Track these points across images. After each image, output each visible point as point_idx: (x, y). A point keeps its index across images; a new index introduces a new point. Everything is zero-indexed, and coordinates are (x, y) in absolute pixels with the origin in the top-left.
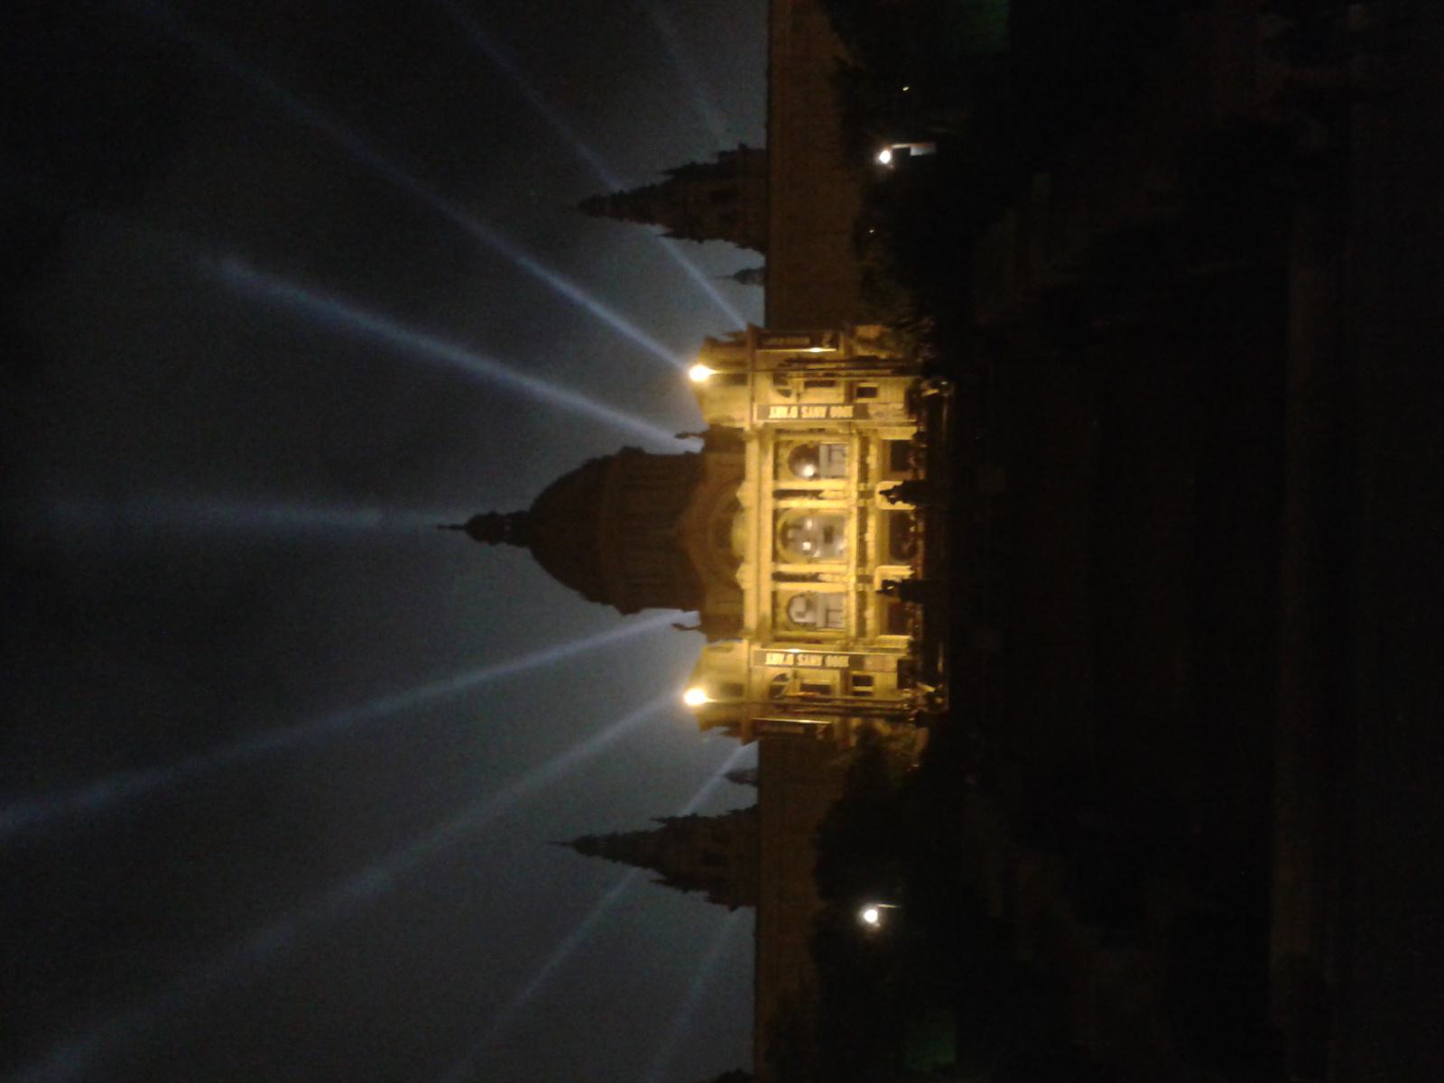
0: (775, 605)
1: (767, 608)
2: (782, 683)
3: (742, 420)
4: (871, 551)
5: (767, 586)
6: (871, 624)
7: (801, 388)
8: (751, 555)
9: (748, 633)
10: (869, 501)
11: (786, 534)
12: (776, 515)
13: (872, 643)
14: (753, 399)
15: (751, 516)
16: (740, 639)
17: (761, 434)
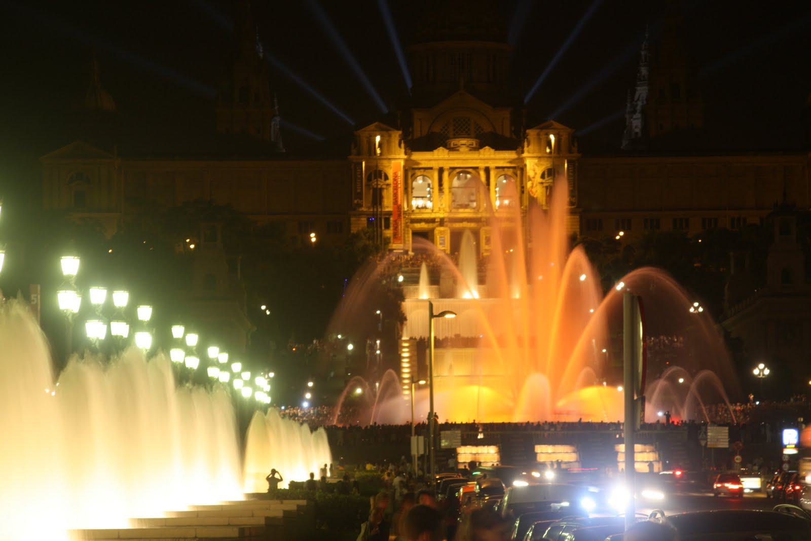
0: (425, 169)
1: (424, 164)
2: (383, 177)
3: (529, 152)
4: (457, 225)
5: (436, 165)
6: (418, 226)
7: (545, 185)
8: (454, 155)
9: (410, 155)
10: (485, 223)
11: (465, 170)
12: (476, 168)
13: (408, 227)
14: (539, 158)
15: (475, 155)
16: (406, 153)
17: (522, 160)
